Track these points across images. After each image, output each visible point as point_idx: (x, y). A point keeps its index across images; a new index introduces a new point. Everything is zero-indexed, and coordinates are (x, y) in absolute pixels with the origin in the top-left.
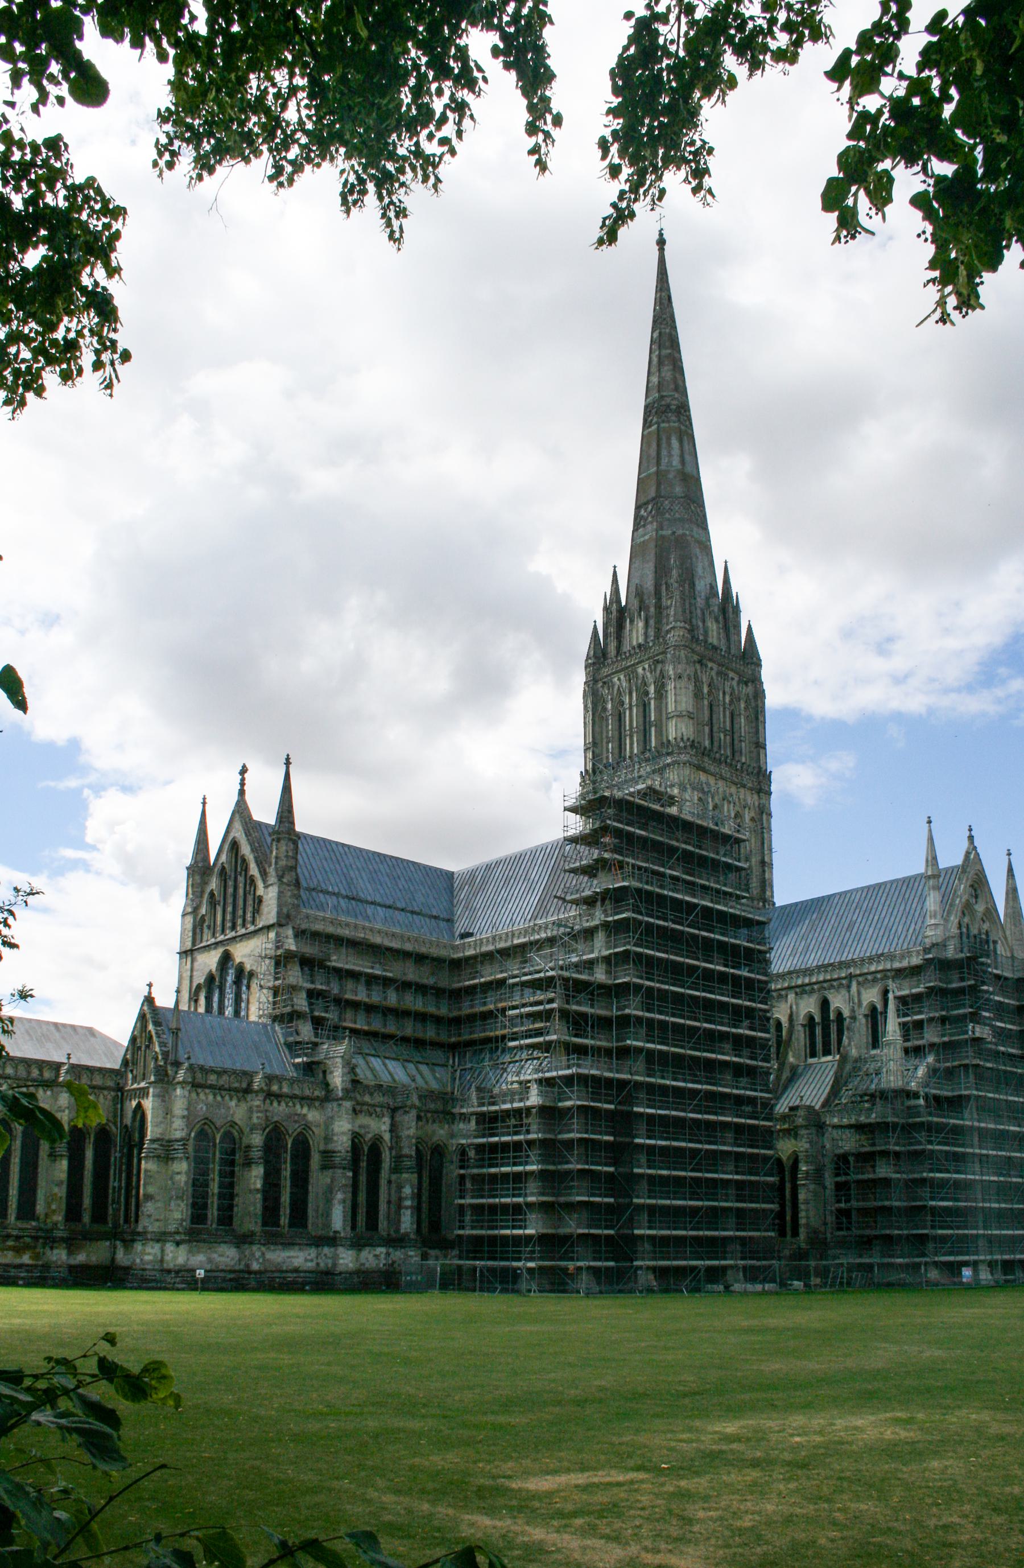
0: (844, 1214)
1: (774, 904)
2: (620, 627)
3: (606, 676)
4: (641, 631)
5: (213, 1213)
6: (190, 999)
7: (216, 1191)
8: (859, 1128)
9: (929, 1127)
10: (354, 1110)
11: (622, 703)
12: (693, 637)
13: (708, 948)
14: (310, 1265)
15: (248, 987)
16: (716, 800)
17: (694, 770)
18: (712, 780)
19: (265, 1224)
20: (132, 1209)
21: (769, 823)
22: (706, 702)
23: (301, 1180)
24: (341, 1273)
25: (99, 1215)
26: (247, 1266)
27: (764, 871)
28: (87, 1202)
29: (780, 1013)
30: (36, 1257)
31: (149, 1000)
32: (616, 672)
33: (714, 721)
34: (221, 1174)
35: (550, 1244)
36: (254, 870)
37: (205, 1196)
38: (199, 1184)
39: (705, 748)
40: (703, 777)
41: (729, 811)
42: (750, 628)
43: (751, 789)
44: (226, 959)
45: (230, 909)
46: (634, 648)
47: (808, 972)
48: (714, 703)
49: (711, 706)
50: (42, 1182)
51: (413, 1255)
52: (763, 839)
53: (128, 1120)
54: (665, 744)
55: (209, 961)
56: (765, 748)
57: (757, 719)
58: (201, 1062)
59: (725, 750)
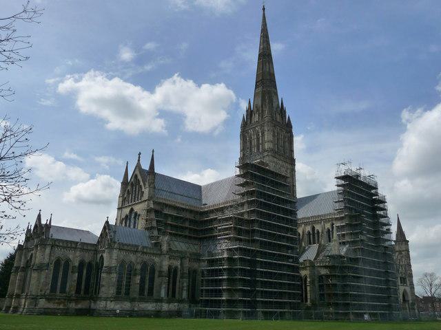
0: (322, 295)
5: (123, 291)
8: (326, 267)
9: (348, 268)
13: (279, 209)
14: (154, 309)
20: (97, 291)
23: (152, 280)
28: (83, 287)
29: (300, 231)
30: (65, 305)
31: (107, 222)
35: (230, 302)
36: (142, 183)
38: (119, 281)
40: (275, 159)
44: (132, 210)
47: (308, 218)
49: (278, 139)
50: (69, 281)
51: (186, 306)
54: (264, 151)
55: (127, 211)
58: (122, 242)
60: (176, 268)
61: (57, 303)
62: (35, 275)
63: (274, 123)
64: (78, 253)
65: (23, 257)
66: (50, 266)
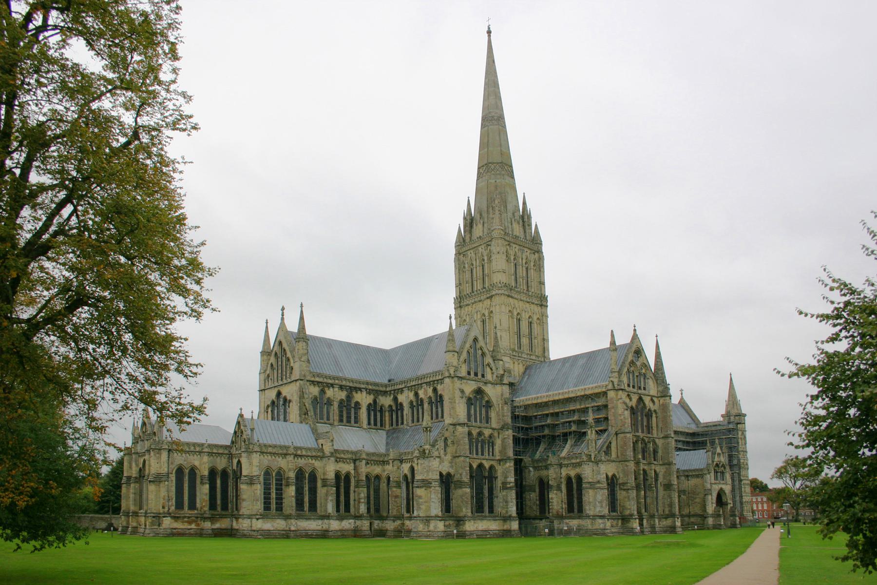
1: (550, 359)
2: (471, 227)
4: (481, 230)
6: (265, 411)
7: (274, 497)
10: (336, 461)
11: (472, 265)
15: (289, 407)
16: (518, 311)
18: (516, 301)
19: (297, 510)
21: (547, 320)
22: (512, 264)
23: (313, 491)
24: (332, 531)
25: (225, 507)
26: (290, 528)
28: (219, 502)
32: (469, 250)
34: (277, 489)
37: (270, 498)
41: (525, 315)
42: (536, 225)
43: (537, 304)
45: (280, 371)
46: (478, 238)
48: (517, 264)
50: (198, 494)
52: (543, 328)
53: (235, 467)
54: (493, 285)
55: (272, 394)
57: (540, 271)
60: (348, 476)
61: (186, 522)
62: (152, 487)
63: (510, 240)
64: (206, 458)
65: (134, 465)
66: (170, 475)
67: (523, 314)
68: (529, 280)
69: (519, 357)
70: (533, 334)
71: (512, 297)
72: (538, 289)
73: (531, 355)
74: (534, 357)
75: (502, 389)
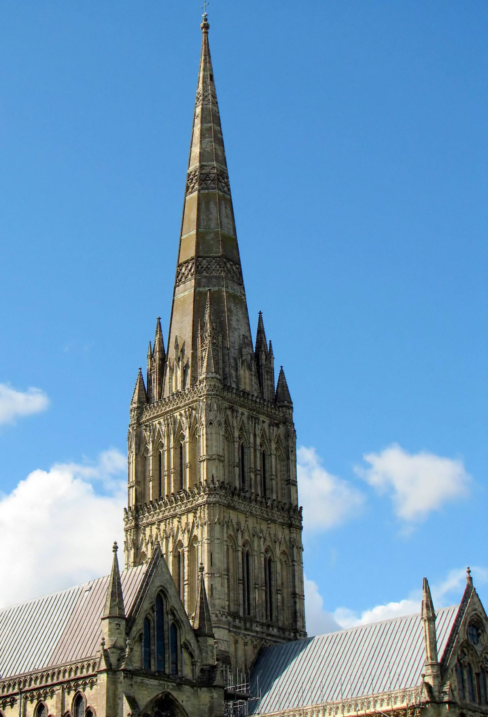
3: (148, 420)
12: (225, 385)
16: (246, 537)
17: (223, 509)
21: (300, 556)
22: (236, 445)
27: (295, 602)
33: (246, 463)
39: (235, 488)
40: (233, 515)
41: (259, 546)
42: (282, 373)
43: (282, 524)
48: (245, 445)
49: (242, 447)
52: (294, 571)
56: (296, 485)
57: (288, 458)
59: (256, 489)
67: (256, 544)
68: (267, 475)
69: (246, 629)
70: (273, 583)
71: (234, 509)
72: (283, 495)
73: (268, 626)
74: (275, 631)
75: (212, 697)
